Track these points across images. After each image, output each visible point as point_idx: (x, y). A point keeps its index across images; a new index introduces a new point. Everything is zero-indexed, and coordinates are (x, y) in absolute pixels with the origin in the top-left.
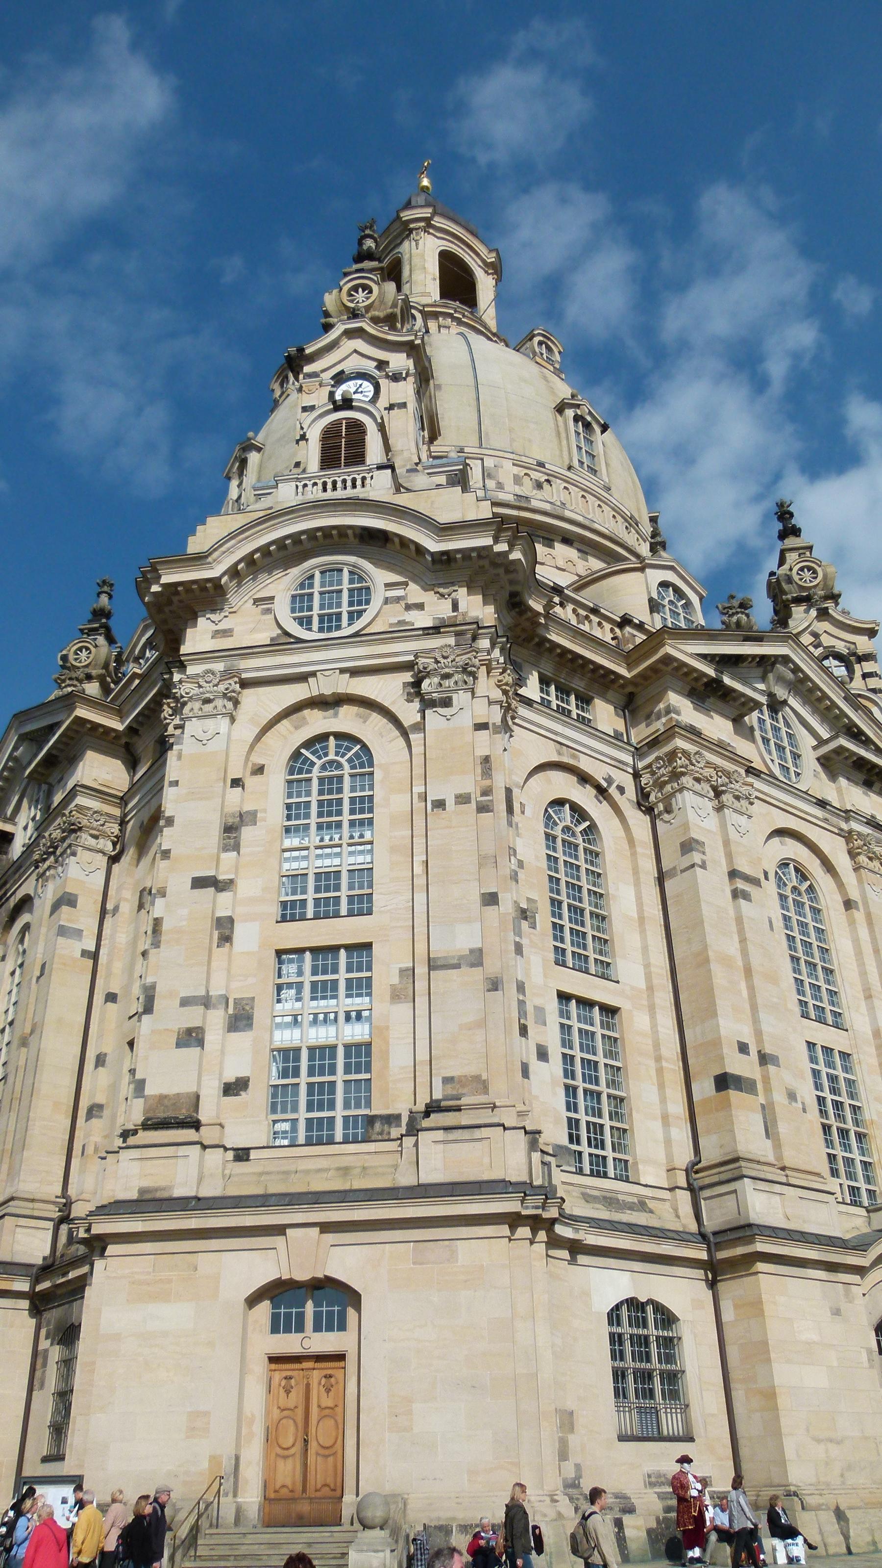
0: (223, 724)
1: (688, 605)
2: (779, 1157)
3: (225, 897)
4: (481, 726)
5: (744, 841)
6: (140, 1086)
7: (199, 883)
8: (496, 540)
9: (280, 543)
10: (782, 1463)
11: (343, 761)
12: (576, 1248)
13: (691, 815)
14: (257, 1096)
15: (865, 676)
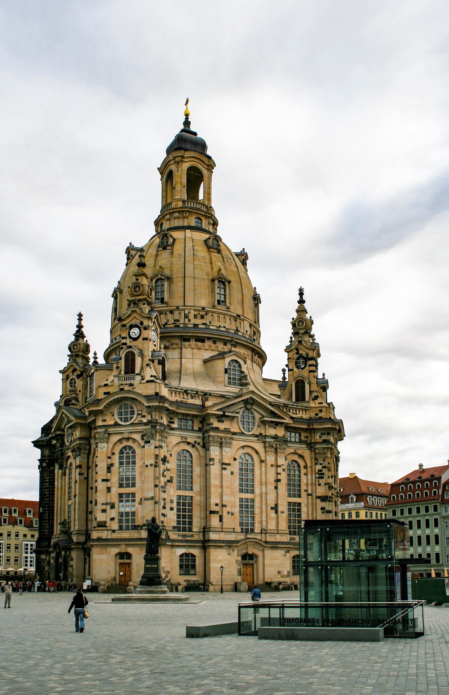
0: (105, 445)
1: (240, 366)
2: (222, 526)
3: (109, 483)
4: (156, 447)
5: (228, 455)
6: (96, 519)
7: (103, 480)
8: (160, 402)
9: (114, 400)
10: (210, 578)
11: (130, 452)
12: (172, 546)
13: (212, 452)
14: (116, 521)
15: (310, 365)
